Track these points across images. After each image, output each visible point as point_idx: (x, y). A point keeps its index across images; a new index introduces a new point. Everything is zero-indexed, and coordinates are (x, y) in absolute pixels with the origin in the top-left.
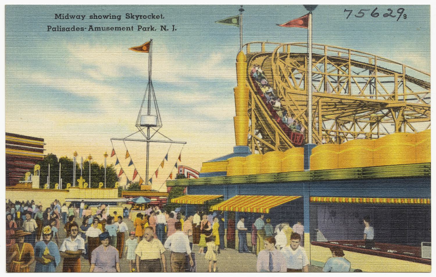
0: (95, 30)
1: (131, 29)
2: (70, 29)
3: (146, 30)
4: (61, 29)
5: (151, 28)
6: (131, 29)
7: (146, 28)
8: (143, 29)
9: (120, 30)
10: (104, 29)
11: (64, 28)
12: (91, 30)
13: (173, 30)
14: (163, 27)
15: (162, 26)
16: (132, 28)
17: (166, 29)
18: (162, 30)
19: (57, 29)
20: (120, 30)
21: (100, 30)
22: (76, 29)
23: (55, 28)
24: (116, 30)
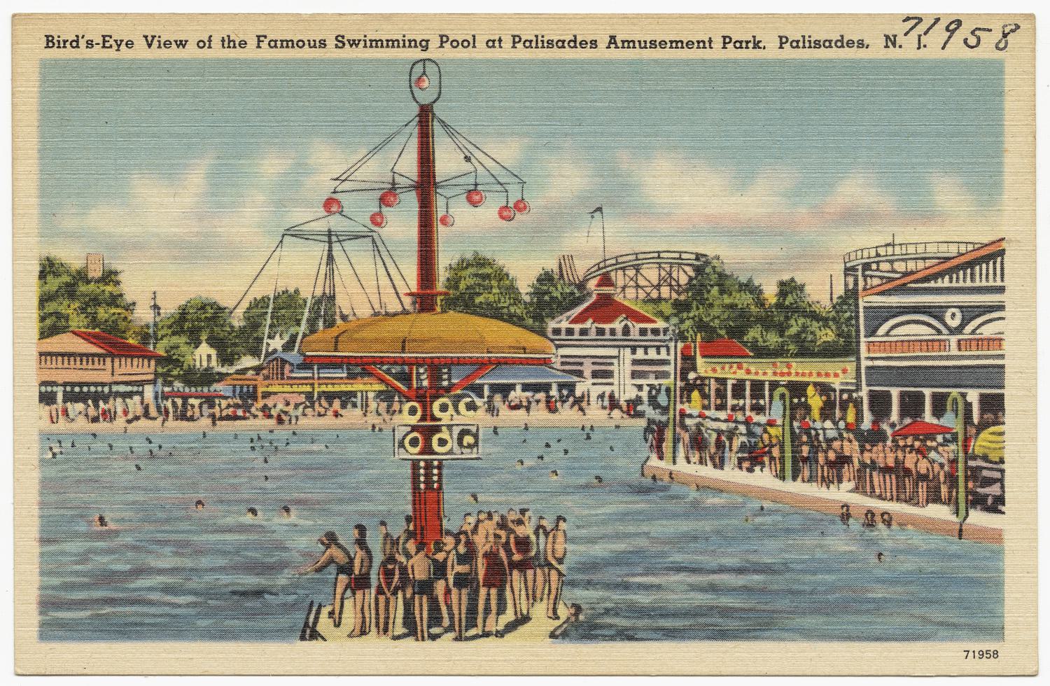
0: (623, 47)
1: (707, 45)
2: (833, 44)
3: (741, 47)
4: (648, 42)
5: (754, 40)
6: (707, 45)
7: (741, 42)
8: (791, 43)
9: (682, 47)
10: (643, 45)
11: (655, 41)
12: (612, 46)
13: (919, 48)
14: (891, 40)
15: (887, 37)
16: (500, 40)
17: (866, 42)
18: (887, 46)
19: (801, 44)
20: (293, 47)
21: (634, 47)
22: (847, 43)
23: (798, 42)
24: (671, 47)
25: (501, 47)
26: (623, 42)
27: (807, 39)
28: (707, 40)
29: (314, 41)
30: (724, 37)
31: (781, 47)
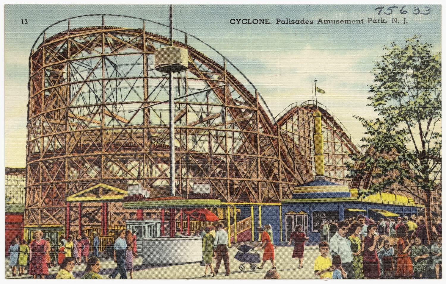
0: (325, 23)
1: (361, 22)
2: (300, 22)
9: (350, 23)
10: (333, 22)
12: (320, 23)
13: (404, 23)
15: (393, 19)
16: (362, 20)
17: (398, 21)
18: (393, 23)
19: (286, 22)
21: (330, 23)
23: (284, 21)
25: (363, 23)
26: (325, 21)
27: (288, 20)
28: (360, 20)
29: (334, 21)
30: (277, 19)
31: (277, 23)
